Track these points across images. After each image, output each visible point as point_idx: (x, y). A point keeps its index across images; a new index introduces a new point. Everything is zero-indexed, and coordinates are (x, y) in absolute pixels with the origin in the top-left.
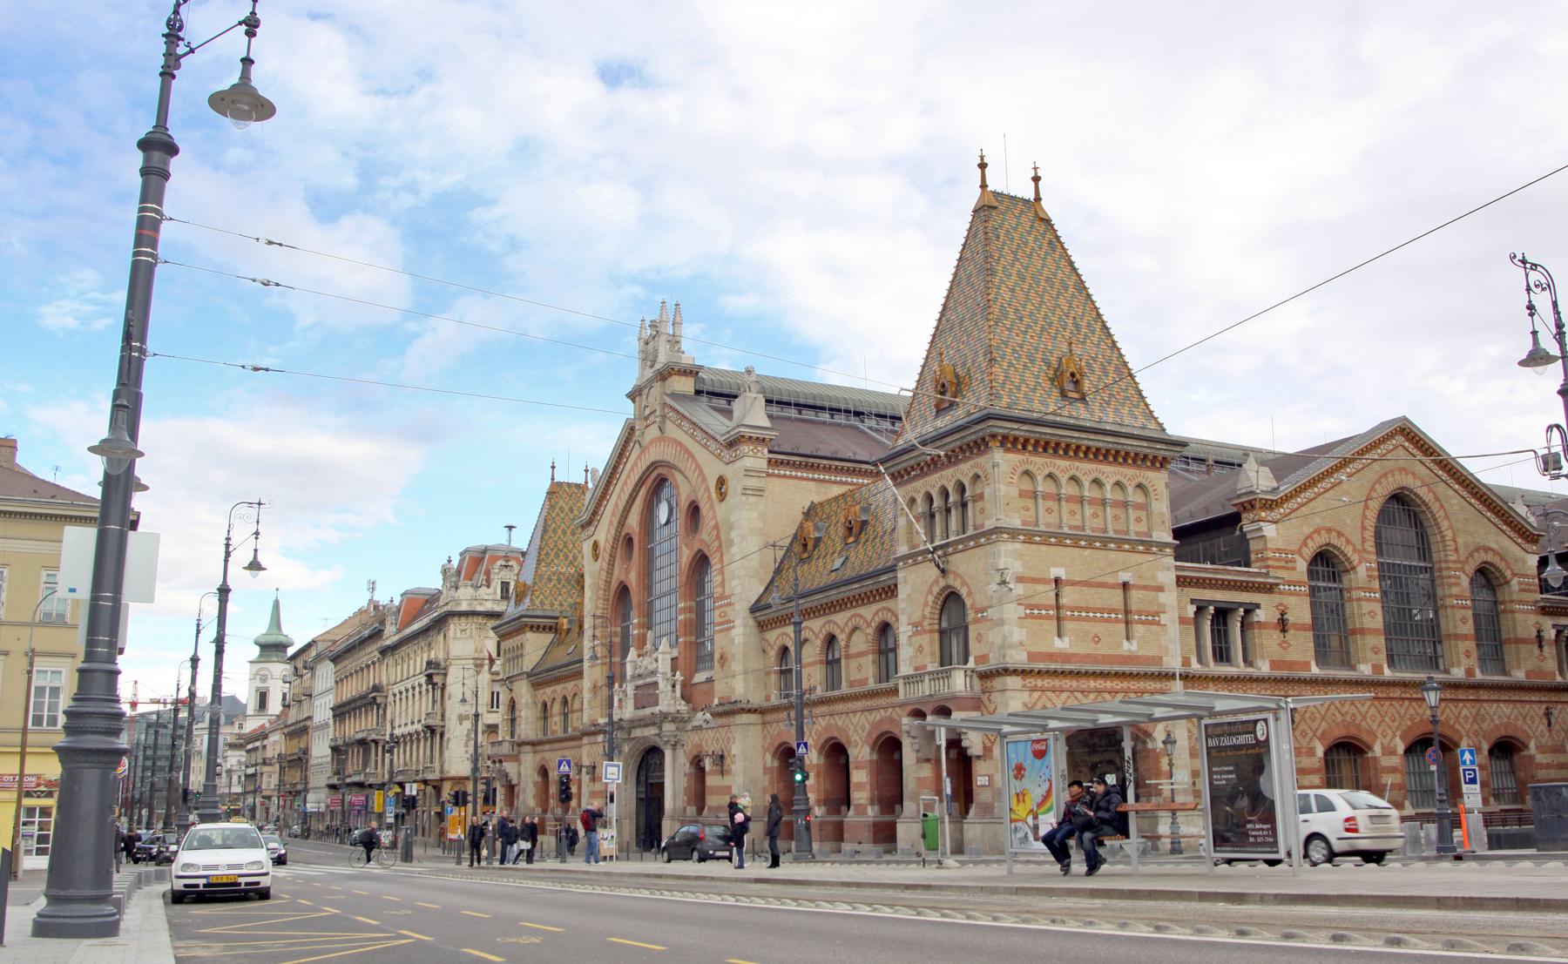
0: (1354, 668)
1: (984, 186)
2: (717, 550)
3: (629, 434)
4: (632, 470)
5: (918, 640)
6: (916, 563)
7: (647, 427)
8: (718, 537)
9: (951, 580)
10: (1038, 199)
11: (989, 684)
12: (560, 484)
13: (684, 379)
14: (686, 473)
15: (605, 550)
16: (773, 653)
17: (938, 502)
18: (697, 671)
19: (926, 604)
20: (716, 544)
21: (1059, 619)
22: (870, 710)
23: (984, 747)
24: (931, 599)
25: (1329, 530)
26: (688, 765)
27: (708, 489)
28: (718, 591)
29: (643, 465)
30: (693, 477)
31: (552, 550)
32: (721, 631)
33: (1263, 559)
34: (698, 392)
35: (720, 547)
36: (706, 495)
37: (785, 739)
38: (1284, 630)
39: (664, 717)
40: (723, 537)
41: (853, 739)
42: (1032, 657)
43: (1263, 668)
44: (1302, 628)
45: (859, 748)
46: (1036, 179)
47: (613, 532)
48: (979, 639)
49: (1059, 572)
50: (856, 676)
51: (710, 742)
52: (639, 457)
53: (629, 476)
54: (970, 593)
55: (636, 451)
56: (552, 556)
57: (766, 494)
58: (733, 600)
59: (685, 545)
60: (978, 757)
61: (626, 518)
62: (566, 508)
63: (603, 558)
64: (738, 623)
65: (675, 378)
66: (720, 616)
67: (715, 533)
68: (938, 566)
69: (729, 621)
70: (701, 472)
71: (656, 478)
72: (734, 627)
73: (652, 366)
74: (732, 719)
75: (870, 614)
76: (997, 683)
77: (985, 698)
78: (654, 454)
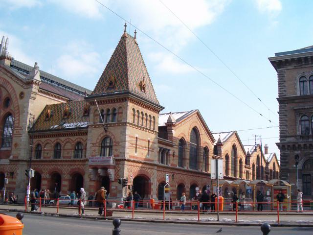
0: (182, 167)
1: (125, 31)
5: (93, 148)
6: (95, 127)
8: (18, 109)
9: (108, 134)
10: (135, 38)
11: (118, 163)
13: (8, 60)
14: (7, 89)
16: (34, 146)
17: (105, 112)
18: (2, 147)
19: (98, 139)
20: (18, 111)
21: (136, 148)
22: (71, 165)
23: (115, 179)
24: (100, 138)
25: (183, 134)
27: (16, 95)
28: (17, 125)
30: (10, 91)
33: (171, 139)
34: (12, 66)
35: (19, 112)
36: (15, 96)
38: (174, 157)
40: (20, 109)
42: (130, 156)
43: (170, 165)
44: (176, 156)
46: (135, 33)
48: (116, 150)
49: (137, 136)
50: (66, 155)
54: (114, 138)
60: (113, 181)
64: (23, 135)
65: (6, 60)
66: (16, 132)
67: (17, 108)
68: (105, 129)
69: (20, 134)
70: (13, 89)
74: (18, 163)
75: (74, 139)
76: (121, 162)
77: (117, 166)
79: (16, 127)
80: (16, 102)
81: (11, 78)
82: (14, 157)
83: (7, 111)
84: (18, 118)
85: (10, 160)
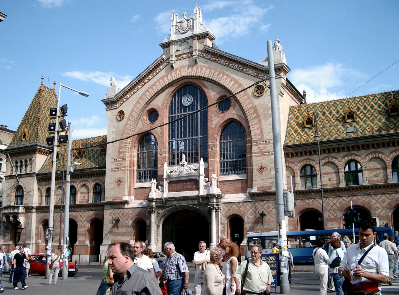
2: (255, 118)
7: (178, 60)
12: (45, 87)
20: (255, 115)
31: (44, 116)
32: (258, 156)
35: (258, 116)
39: (213, 196)
41: (375, 206)
45: (380, 210)
47: (140, 107)
53: (158, 81)
56: (44, 120)
57: (283, 96)
61: (151, 101)
62: (48, 99)
63: (129, 119)
65: (208, 39)
66: (259, 148)
67: (252, 111)
71: (184, 83)
73: (185, 33)
80: (248, 102)
83: (228, 118)
84: (257, 126)
85: (252, 195)
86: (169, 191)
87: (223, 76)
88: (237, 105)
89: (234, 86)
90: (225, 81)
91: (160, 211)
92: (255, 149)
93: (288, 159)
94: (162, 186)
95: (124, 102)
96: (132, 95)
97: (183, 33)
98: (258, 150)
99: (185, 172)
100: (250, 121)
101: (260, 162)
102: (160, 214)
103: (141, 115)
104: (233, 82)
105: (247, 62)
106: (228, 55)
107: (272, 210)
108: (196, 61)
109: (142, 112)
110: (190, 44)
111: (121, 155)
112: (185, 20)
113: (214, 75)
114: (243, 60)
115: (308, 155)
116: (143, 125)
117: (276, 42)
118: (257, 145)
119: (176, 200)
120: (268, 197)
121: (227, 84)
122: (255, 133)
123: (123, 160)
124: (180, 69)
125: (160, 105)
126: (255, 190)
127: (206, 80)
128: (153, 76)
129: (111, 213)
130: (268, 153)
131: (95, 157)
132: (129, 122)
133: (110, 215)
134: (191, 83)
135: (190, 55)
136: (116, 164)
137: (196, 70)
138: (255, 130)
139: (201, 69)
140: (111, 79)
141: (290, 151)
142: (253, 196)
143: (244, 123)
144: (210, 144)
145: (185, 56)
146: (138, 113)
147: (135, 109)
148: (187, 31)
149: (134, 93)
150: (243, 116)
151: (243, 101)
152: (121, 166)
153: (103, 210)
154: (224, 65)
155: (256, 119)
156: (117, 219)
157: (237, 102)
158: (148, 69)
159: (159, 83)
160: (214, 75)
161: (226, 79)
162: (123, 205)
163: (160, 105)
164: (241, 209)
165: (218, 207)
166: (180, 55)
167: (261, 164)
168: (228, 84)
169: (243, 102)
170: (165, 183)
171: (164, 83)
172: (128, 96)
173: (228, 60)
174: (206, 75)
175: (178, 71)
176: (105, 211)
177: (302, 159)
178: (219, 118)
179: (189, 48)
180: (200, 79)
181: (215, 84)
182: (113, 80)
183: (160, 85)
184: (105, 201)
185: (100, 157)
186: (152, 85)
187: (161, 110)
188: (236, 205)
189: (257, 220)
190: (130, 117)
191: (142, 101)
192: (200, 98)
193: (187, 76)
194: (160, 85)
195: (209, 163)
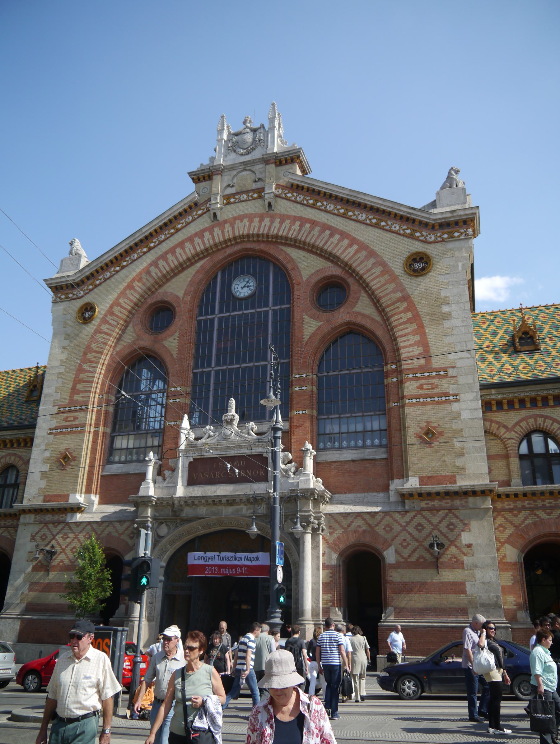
2: (409, 321)
3: (190, 207)
4: (190, 239)
7: (229, 203)
15: (110, 312)
16: (511, 436)
20: (409, 315)
26: (335, 556)
27: (383, 264)
29: (218, 235)
32: (417, 404)
35: (416, 318)
36: (378, 270)
37: (554, 529)
40: (422, 309)
47: (134, 296)
51: (397, 528)
52: (210, 230)
53: (181, 244)
55: (205, 222)
58: (451, 372)
59: (311, 317)
61: (160, 286)
63: (104, 321)
64: (462, 396)
66: (421, 387)
69: (447, 395)
70: (363, 246)
71: (240, 251)
72: (458, 401)
73: (248, 153)
74: (457, 502)
78: (242, 228)
79: (413, 371)
80: (391, 286)
81: (344, 216)
82: (422, 480)
85: (405, 496)
86: (191, 482)
87: (331, 235)
88: (363, 293)
89: (359, 255)
90: (337, 244)
91: (163, 530)
92: (410, 388)
93: (490, 415)
94: (174, 470)
95: (96, 286)
96: (117, 272)
97: (242, 155)
98: (420, 392)
99: (233, 438)
100: (396, 326)
101: (425, 418)
102: (163, 537)
103: (133, 315)
104: (355, 247)
105: (389, 207)
106: (345, 192)
107: (459, 535)
108: (270, 205)
109: (136, 308)
110: (257, 173)
111: (76, 397)
112: (248, 130)
113: (310, 233)
114: (380, 202)
115: (540, 407)
116: (138, 336)
117: (453, 172)
118: (415, 379)
119: (207, 504)
120: (449, 501)
121: (340, 251)
122: (409, 352)
123: (80, 410)
124: (232, 222)
125: (181, 294)
126: (413, 483)
127: (290, 245)
128: (168, 233)
129: (37, 533)
130: (444, 398)
131: (14, 408)
132: (104, 328)
133: (33, 538)
134: (254, 250)
135: (256, 195)
136: (62, 418)
137: (268, 224)
138: (411, 345)
139: (281, 223)
140: (72, 242)
141: (493, 397)
142: (408, 499)
143: (380, 333)
144: (298, 376)
145: (245, 196)
146: (129, 308)
147: (121, 301)
148: (254, 149)
149: (123, 268)
150: (378, 318)
151: (379, 285)
152: (74, 423)
153: (16, 527)
154: (334, 214)
155: (411, 323)
156: (48, 548)
157: (364, 288)
158: (160, 219)
159: (183, 248)
160: (310, 233)
161: (339, 241)
162: (69, 515)
163: (181, 294)
164: (380, 530)
165: (319, 524)
166: (233, 195)
167: (428, 422)
168: (344, 251)
169: (378, 288)
170: (182, 464)
171: (194, 248)
172: (108, 274)
173: (344, 204)
174: (291, 232)
175: (227, 226)
176: (20, 528)
177: (524, 416)
178: (321, 321)
179: (255, 181)
180: (276, 243)
181: (311, 252)
182: (77, 244)
183: (185, 252)
184: (25, 503)
185: (24, 406)
186: (166, 253)
187: (182, 305)
188: (364, 519)
189: (422, 560)
190: (109, 318)
191: (140, 285)
192: (274, 283)
193: (248, 236)
194: (185, 252)
195: (295, 420)
